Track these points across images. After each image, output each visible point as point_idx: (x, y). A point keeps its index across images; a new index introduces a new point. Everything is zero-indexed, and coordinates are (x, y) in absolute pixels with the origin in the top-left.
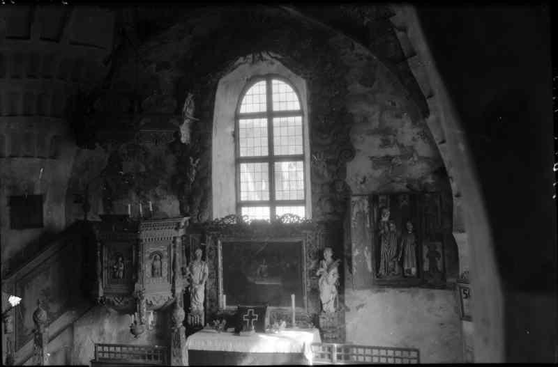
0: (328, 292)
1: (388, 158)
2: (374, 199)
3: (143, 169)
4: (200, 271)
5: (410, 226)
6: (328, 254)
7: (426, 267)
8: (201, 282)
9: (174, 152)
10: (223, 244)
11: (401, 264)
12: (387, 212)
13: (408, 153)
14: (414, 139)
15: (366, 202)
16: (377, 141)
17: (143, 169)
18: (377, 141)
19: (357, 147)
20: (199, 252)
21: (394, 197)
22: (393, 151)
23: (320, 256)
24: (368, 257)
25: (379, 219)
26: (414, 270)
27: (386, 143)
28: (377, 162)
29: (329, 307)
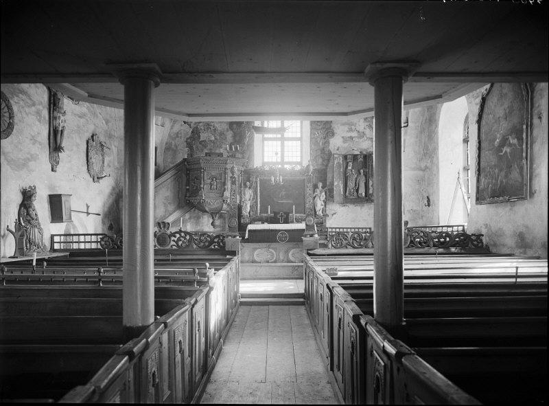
0: (319, 205)
1: (351, 138)
2: (345, 157)
3: (213, 138)
4: (248, 193)
5: (362, 171)
6: (320, 185)
7: (371, 192)
8: (250, 200)
9: (232, 130)
10: (261, 180)
11: (357, 191)
12: (351, 164)
13: (362, 135)
14: (365, 128)
15: (341, 160)
16: (346, 128)
17: (213, 138)
18: (346, 128)
19: (335, 131)
20: (248, 183)
21: (355, 157)
22: (354, 134)
23: (315, 187)
24: (342, 186)
25: (347, 167)
26: (364, 194)
27: (351, 130)
28: (345, 140)
29: (320, 213)
